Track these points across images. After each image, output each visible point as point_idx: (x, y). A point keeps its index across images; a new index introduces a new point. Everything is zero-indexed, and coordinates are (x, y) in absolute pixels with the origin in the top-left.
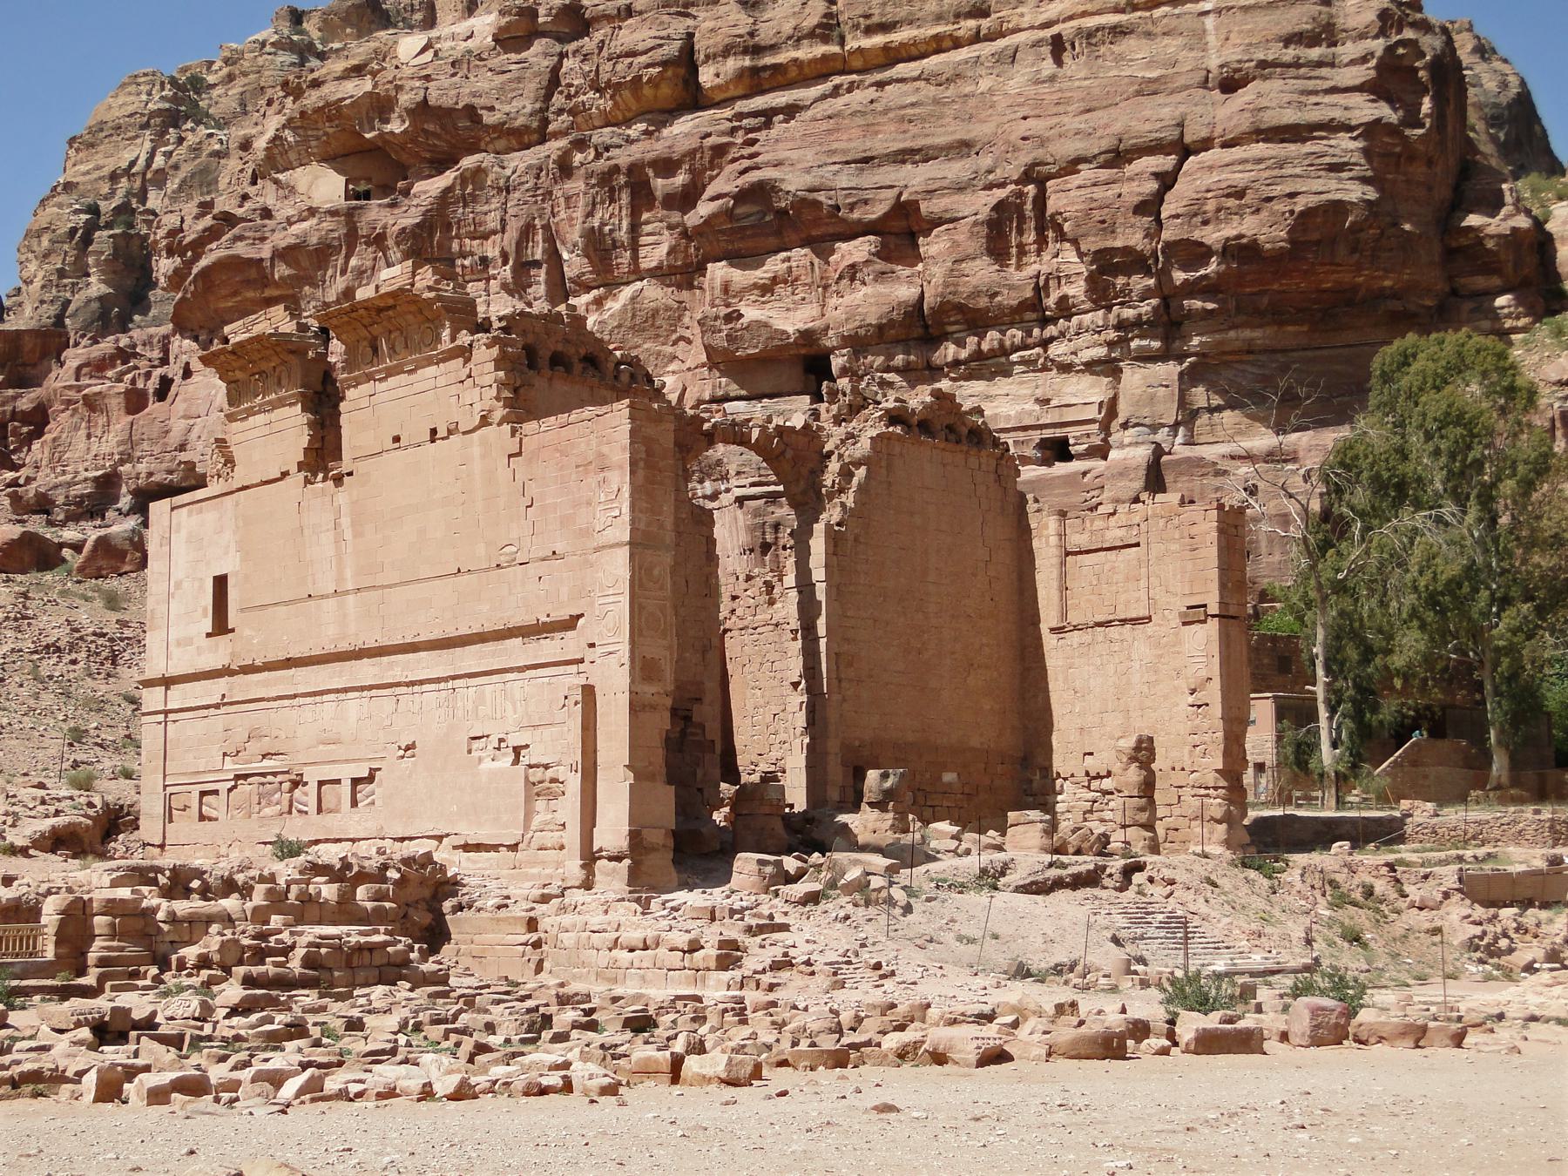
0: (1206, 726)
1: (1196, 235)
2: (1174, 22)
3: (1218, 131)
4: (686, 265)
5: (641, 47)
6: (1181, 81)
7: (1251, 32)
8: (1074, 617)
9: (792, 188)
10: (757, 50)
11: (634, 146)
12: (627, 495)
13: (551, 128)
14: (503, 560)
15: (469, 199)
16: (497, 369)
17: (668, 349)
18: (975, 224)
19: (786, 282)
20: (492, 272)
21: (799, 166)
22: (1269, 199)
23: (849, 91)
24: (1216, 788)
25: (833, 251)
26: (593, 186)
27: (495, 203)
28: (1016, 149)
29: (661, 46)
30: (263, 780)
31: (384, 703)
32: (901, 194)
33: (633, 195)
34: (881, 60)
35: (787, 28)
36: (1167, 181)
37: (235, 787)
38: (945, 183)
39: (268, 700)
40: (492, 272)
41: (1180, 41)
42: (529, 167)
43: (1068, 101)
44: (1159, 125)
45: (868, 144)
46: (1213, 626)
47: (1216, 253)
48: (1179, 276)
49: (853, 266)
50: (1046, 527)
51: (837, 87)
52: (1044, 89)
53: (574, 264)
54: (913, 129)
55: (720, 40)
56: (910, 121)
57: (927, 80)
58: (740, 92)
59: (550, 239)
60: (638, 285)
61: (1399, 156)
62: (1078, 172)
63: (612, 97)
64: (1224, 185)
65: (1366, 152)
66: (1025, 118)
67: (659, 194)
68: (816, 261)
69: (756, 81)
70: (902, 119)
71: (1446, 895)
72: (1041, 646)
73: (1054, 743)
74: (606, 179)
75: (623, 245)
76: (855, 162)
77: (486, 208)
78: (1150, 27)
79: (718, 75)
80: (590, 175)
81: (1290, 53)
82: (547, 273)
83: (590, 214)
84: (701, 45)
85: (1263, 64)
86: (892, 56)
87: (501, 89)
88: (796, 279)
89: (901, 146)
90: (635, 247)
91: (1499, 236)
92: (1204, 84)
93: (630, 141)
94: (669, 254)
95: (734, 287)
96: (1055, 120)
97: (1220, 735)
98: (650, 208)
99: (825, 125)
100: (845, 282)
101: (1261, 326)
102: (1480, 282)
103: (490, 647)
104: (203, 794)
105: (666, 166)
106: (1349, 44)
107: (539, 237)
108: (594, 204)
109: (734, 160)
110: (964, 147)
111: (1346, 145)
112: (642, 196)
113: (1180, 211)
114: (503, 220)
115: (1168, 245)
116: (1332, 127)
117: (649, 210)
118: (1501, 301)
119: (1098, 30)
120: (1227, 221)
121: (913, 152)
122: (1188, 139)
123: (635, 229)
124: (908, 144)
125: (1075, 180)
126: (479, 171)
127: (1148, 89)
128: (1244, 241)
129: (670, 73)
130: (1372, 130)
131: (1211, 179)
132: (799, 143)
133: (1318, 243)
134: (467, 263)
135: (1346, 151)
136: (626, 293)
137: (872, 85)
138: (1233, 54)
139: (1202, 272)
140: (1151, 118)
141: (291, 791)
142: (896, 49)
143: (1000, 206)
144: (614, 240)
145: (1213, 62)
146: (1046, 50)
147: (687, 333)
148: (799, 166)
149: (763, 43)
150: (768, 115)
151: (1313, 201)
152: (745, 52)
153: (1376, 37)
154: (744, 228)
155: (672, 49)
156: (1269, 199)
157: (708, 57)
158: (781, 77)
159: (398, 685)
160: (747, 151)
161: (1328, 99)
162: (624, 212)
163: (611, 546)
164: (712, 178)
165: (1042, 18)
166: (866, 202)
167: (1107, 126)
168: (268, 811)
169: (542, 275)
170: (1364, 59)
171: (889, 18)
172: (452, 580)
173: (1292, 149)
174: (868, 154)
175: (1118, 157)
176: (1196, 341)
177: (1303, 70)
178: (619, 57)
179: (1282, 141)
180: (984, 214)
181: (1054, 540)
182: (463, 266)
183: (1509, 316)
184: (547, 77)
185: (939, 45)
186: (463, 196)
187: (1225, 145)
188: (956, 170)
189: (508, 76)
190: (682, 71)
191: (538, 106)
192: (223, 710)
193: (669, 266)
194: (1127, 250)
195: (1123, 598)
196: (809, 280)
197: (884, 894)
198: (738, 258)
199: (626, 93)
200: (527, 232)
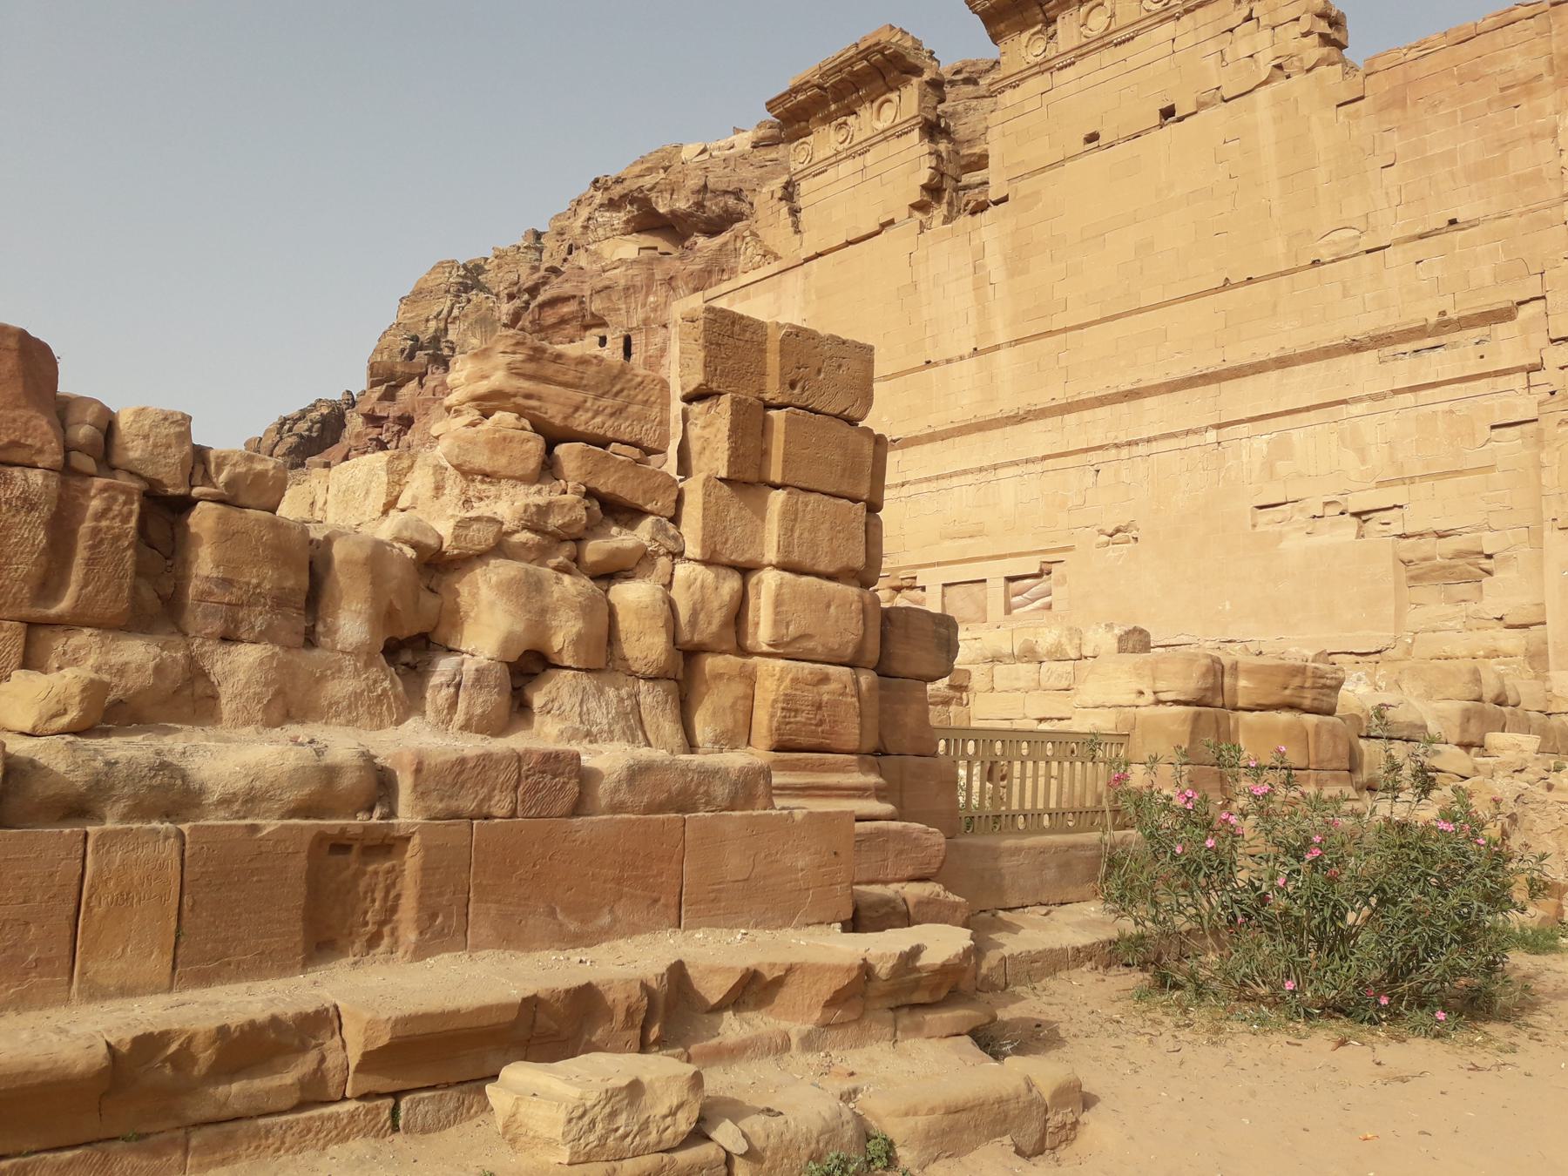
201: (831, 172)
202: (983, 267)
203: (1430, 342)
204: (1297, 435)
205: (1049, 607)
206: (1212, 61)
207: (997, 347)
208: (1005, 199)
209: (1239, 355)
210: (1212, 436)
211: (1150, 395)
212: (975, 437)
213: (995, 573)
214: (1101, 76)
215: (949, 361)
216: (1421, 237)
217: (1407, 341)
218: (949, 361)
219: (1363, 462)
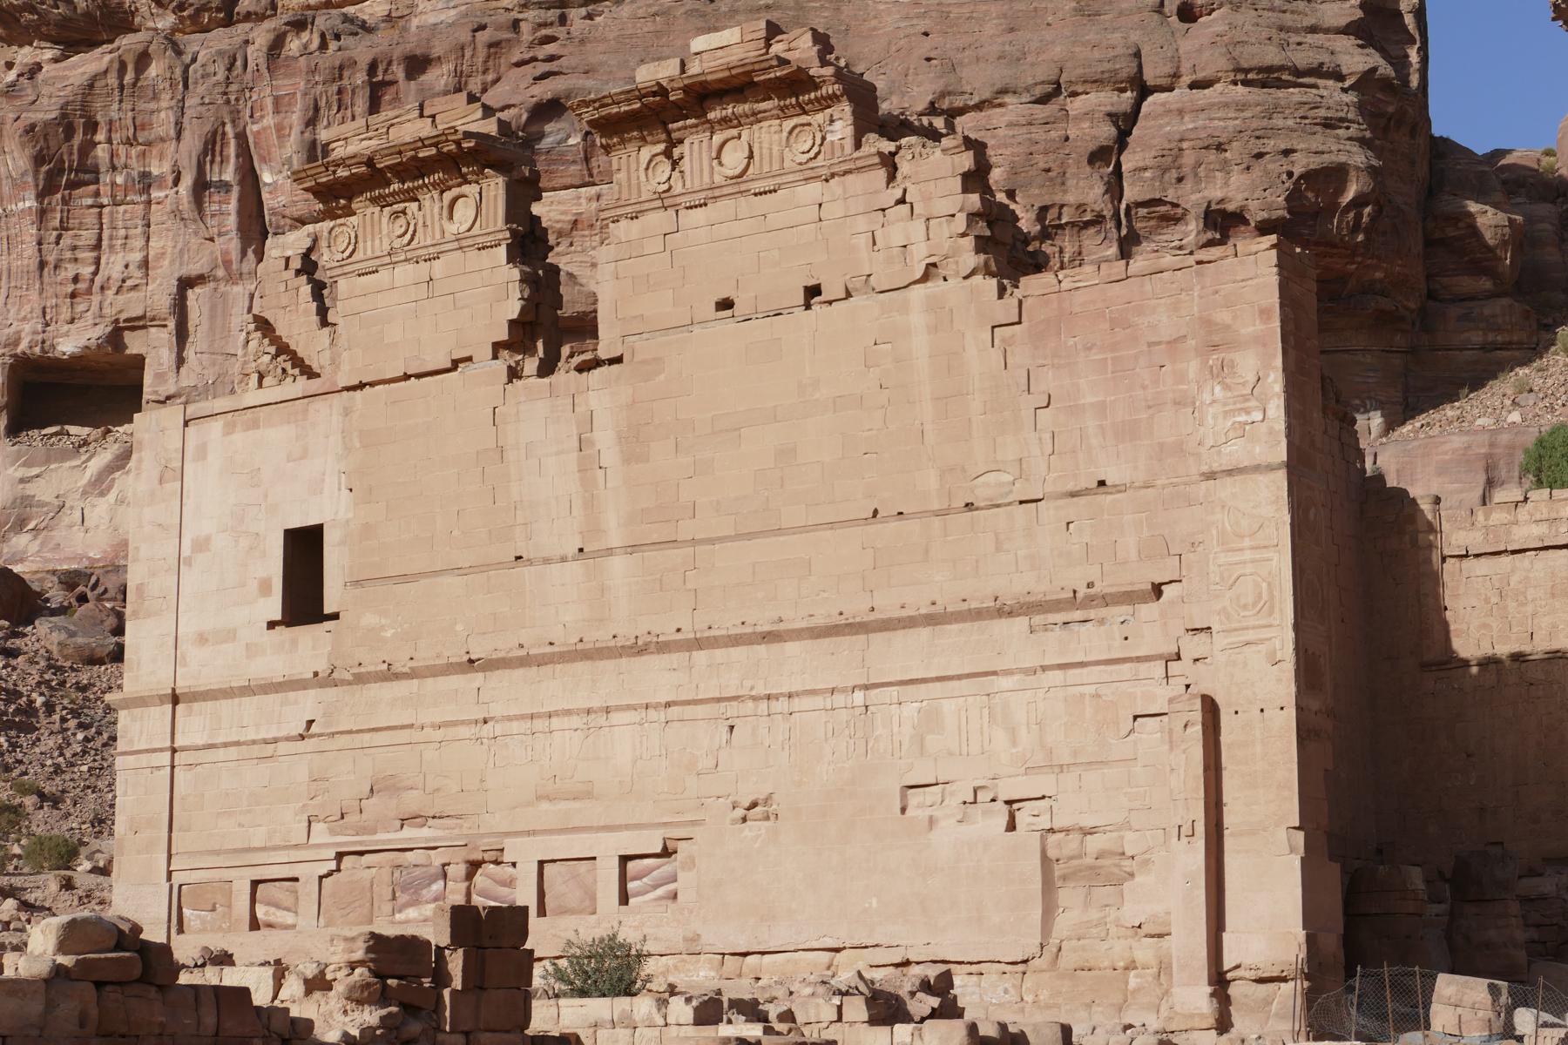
22: (1259, 156)
36: (1125, 123)
44: (1111, 53)
82: (240, 200)
130: (1366, 81)
151: (1315, 163)
156: (1259, 156)
187: (1194, 86)
201: (384, 275)
202: (592, 443)
203: (1078, 615)
204: (948, 707)
205: (675, 896)
206: (864, 240)
207: (610, 551)
208: (618, 360)
209: (888, 605)
210: (859, 696)
211: (792, 639)
212: (581, 667)
213: (608, 849)
214: (738, 228)
215: (547, 561)
216: (1073, 495)
217: (1059, 610)
218: (547, 561)
219: (1014, 743)
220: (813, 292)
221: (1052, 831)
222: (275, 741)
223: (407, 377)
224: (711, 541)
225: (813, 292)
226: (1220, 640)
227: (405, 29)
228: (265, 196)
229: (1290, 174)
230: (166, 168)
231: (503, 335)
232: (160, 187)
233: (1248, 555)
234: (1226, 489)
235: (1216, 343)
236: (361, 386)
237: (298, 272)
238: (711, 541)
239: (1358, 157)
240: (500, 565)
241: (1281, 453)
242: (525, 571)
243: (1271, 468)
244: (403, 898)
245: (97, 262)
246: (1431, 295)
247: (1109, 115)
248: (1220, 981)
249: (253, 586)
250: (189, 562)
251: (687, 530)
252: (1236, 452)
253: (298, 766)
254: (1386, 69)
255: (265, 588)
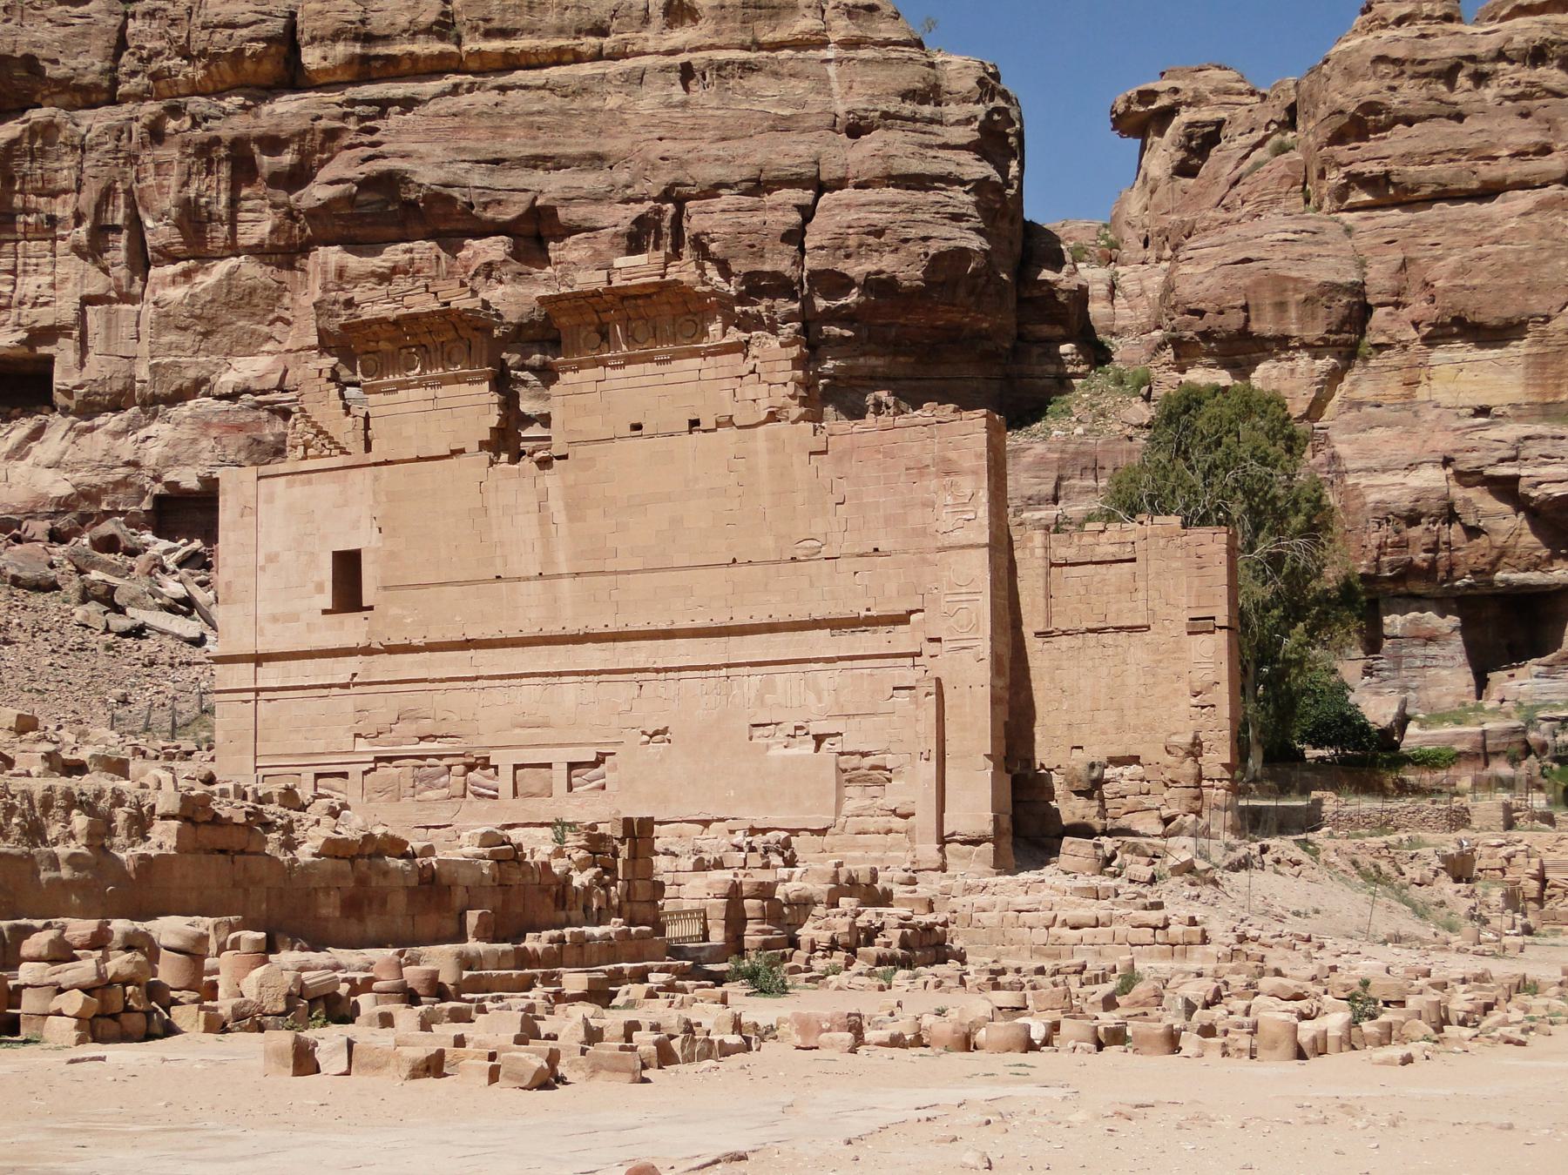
0: (1211, 725)
1: (841, 267)
2: (800, 67)
3: (853, 172)
4: (288, 246)
5: (240, 19)
6: (812, 122)
7: (872, 84)
8: (1059, 623)
9: (426, 181)
10: (368, 39)
11: (232, 119)
12: (985, 500)
13: (122, 89)
14: (799, 554)
15: (37, 154)
16: (794, 368)
17: (265, 329)
18: (616, 235)
19: (406, 272)
20: (59, 232)
21: (431, 160)
22: (906, 241)
23: (469, 91)
24: (1220, 780)
25: (461, 247)
26: (189, 156)
27: (68, 161)
28: (654, 168)
29: (264, 21)
30: (420, 762)
31: (623, 690)
32: (535, 199)
33: (233, 169)
34: (498, 65)
35: (403, 20)
36: (807, 212)
37: (374, 770)
38: (582, 193)
39: (433, 681)
40: (59, 232)
41: (806, 84)
42: (109, 128)
43: (703, 128)
44: (798, 161)
45: (498, 146)
46: (1222, 637)
47: (858, 285)
48: (821, 304)
49: (489, 264)
50: (1031, 539)
51: (456, 86)
52: (677, 113)
53: (159, 232)
54: (543, 137)
55: (329, 24)
56: (539, 129)
57: (552, 90)
58: (346, 78)
59: (132, 205)
60: (234, 261)
61: (997, 211)
62: (719, 196)
63: (205, 67)
64: (864, 223)
65: (976, 204)
66: (660, 139)
67: (265, 171)
68: (443, 255)
69: (365, 69)
70: (531, 125)
71: (1436, 874)
72: (1024, 648)
73: (1038, 737)
74: (205, 150)
75: (220, 219)
76: (487, 162)
77: (56, 165)
78: (776, 67)
79: (325, 58)
80: (186, 144)
81: (908, 108)
82: (128, 240)
83: (186, 184)
84: (306, 27)
85: (886, 115)
86: (510, 62)
87: (64, 41)
88: (418, 271)
89: (533, 151)
90: (233, 222)
91: (1070, 291)
92: (832, 127)
93: (228, 114)
94: (272, 232)
95: (350, 273)
96: (692, 144)
97: (1227, 733)
98: (251, 182)
99: (450, 123)
100: (480, 279)
101: (883, 356)
102: (1046, 330)
103: (798, 636)
104: (318, 776)
105: (273, 144)
106: (952, 105)
107: (121, 201)
108: (189, 175)
109: (351, 147)
110: (596, 160)
111: (962, 198)
112: (243, 170)
113: (825, 243)
114: (79, 180)
115: (812, 273)
116: (950, 180)
117: (249, 186)
118: (1065, 348)
119: (728, 63)
120: (867, 257)
121: (545, 158)
122: (823, 177)
123: (234, 203)
124: (539, 151)
125: (718, 204)
126: (48, 130)
127: (782, 125)
128: (884, 276)
129: (273, 50)
130: (980, 186)
131: (852, 216)
132: (422, 137)
133: (943, 284)
134: (31, 220)
135: (963, 203)
136: (221, 268)
137: (494, 88)
138: (859, 103)
139: (843, 302)
140: (792, 153)
141: (465, 775)
142: (517, 56)
143: (640, 221)
144: (210, 213)
145: (841, 108)
146: (675, 76)
147: (287, 315)
148: (431, 160)
149: (376, 33)
150: (384, 105)
151: (944, 246)
152: (356, 38)
153: (977, 102)
154: (365, 215)
155: (276, 26)
156: (906, 241)
157: (313, 39)
158: (393, 69)
159: (645, 670)
160: (366, 138)
161: (942, 153)
162: (223, 186)
163: (963, 547)
164: (322, 163)
165: (666, 46)
166: (499, 202)
167: (745, 156)
168: (430, 794)
169: (122, 240)
170: (968, 121)
171: (509, 25)
172: (724, 570)
173: (919, 196)
174: (499, 156)
175: (759, 186)
176: (830, 364)
177: (918, 125)
178: (216, 26)
179: (908, 188)
180: (625, 225)
181: (1039, 552)
182: (26, 223)
183: (1071, 363)
184: (115, 35)
185: (559, 57)
186: (31, 149)
187: (857, 186)
188: (591, 181)
189: (70, 29)
190: (284, 49)
191: (107, 64)
192: (353, 690)
193: (271, 245)
194: (775, 275)
195: (1114, 608)
196: (433, 273)
197: (1210, 875)
198: (353, 244)
199: (224, 65)
200: (107, 194)
205: (603, 787)
206: (727, 394)
207: (560, 576)
209: (741, 619)
213: (560, 758)
214: (645, 381)
219: (820, 701)
220: (694, 423)
221: (842, 754)
222: (330, 686)
223: (419, 459)
224: (628, 573)
225: (694, 423)
226: (946, 646)
227: (257, 116)
228: (148, 237)
229: (926, 254)
230: (69, 212)
231: (487, 437)
232: (64, 228)
233: (964, 597)
234: (953, 556)
235: (948, 470)
236: (387, 463)
237: (329, 380)
238: (628, 573)
239: (976, 243)
240: (485, 581)
241: (985, 538)
242: (502, 585)
243: (978, 546)
244: (421, 786)
245: (14, 284)
246: (1020, 337)
247: (796, 206)
248: (943, 841)
249: (311, 586)
250: (263, 568)
251: (610, 566)
252: (959, 537)
253: (347, 703)
254: (998, 178)
255: (320, 588)
